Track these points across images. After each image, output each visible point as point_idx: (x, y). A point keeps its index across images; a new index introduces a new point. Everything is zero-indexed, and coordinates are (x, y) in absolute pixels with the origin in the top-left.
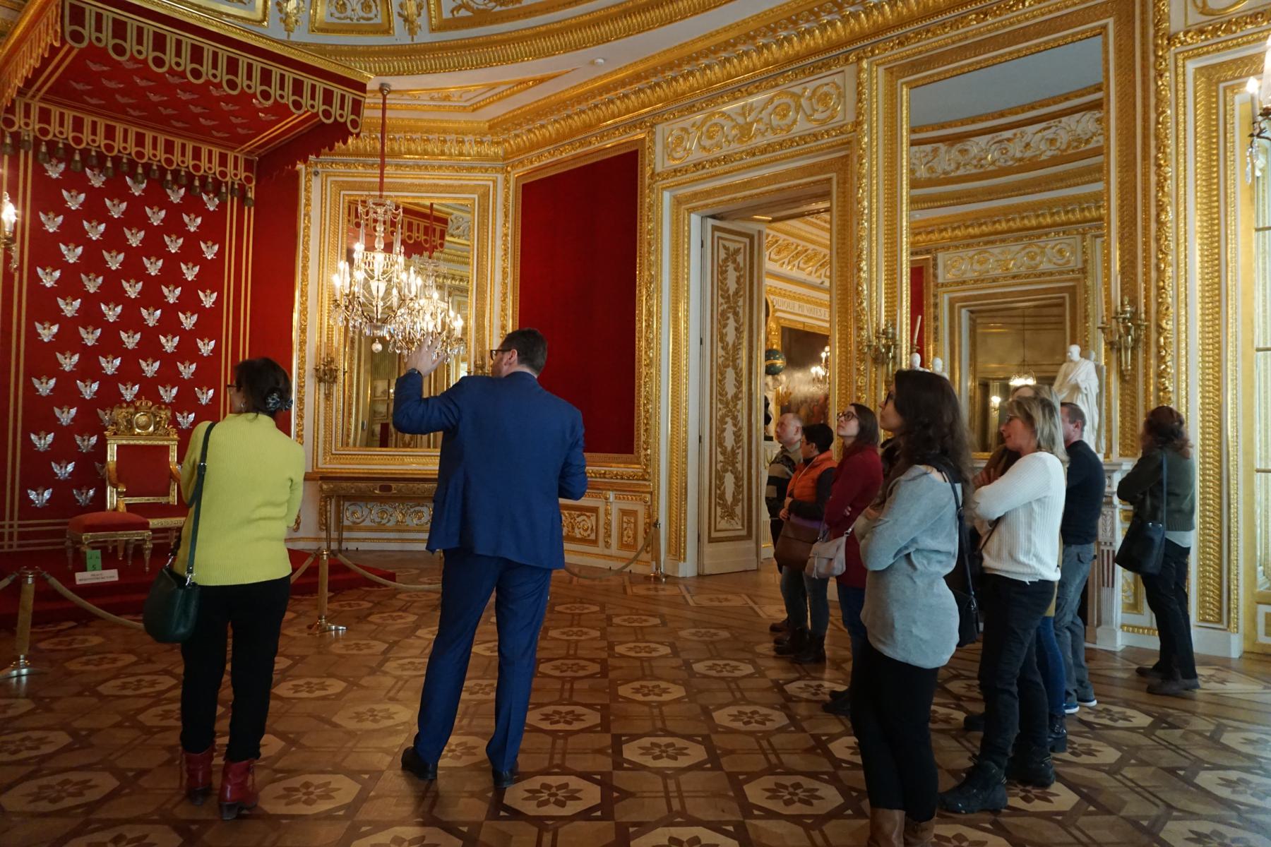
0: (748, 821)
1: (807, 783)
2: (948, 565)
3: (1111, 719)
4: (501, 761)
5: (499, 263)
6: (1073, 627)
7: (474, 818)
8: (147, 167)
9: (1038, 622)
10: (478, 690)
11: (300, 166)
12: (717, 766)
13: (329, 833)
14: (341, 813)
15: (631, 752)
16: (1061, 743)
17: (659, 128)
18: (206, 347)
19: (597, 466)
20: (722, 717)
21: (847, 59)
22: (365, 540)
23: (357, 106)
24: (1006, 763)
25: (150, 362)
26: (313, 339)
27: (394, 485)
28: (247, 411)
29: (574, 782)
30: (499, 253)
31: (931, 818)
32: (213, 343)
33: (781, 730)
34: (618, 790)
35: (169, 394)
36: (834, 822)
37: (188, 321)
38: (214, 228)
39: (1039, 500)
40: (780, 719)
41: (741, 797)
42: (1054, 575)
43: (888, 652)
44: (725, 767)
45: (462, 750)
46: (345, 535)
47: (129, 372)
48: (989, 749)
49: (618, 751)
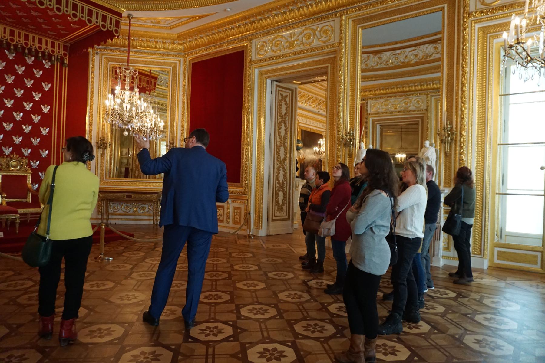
0: (297, 341)
1: (321, 323)
2: (386, 232)
3: (441, 295)
4: (188, 317)
5: (181, 98)
6: (427, 258)
7: (177, 342)
8: (16, 46)
9: (415, 256)
10: (179, 286)
11: (90, 50)
12: (282, 318)
13: (110, 351)
14: (117, 341)
15: (244, 312)
16: (422, 305)
17: (254, 41)
18: (45, 131)
19: (232, 188)
20: (282, 296)
21: (336, 15)
22: (119, 219)
23: (118, 24)
24: (402, 313)
25: (17, 137)
26: (95, 129)
27: (132, 195)
28: (73, 160)
29: (220, 326)
30: (181, 93)
31: (375, 337)
32: (48, 129)
33: (307, 301)
34: (241, 328)
35: (27, 152)
36: (333, 340)
37: (36, 119)
38: (48, 76)
39: (416, 204)
40: (306, 297)
41: (293, 330)
42: (422, 236)
43: (362, 268)
44: (285, 317)
45: (171, 312)
46: (110, 217)
48: (395, 308)
49: (238, 312)
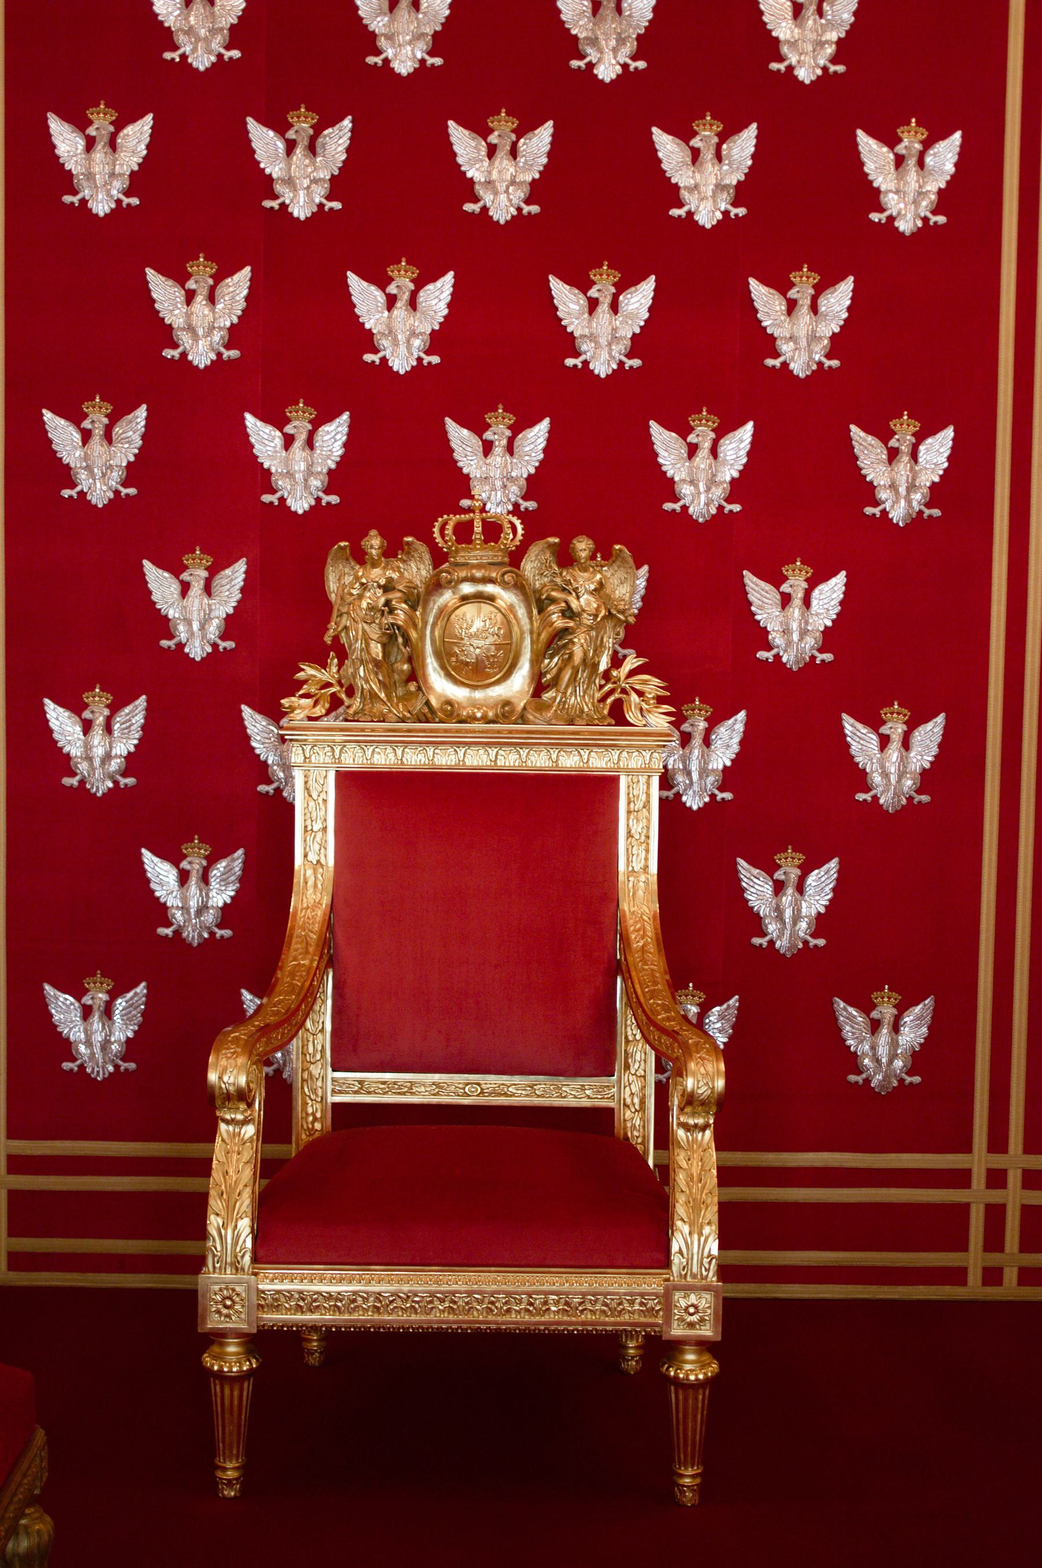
47: (501, 356)
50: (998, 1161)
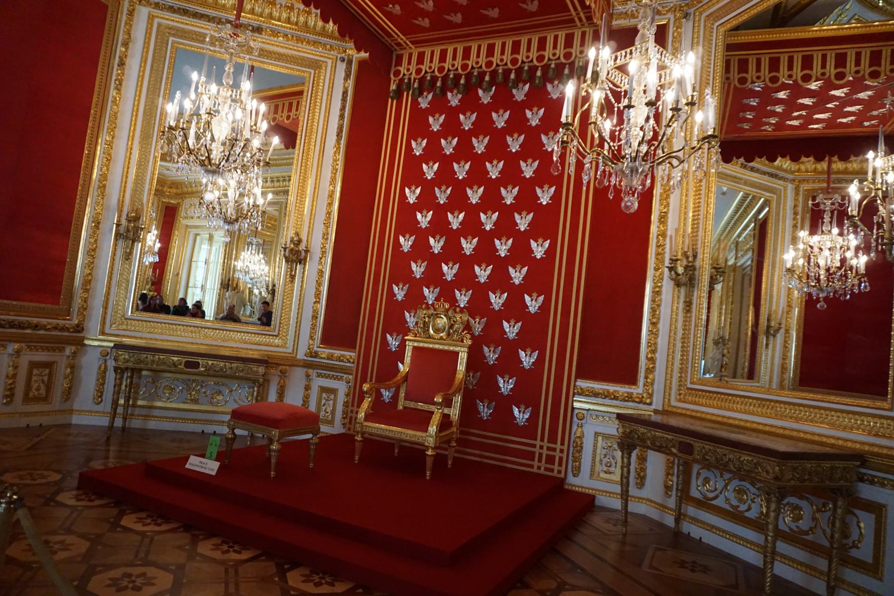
22: (712, 528)
50: (542, 444)
